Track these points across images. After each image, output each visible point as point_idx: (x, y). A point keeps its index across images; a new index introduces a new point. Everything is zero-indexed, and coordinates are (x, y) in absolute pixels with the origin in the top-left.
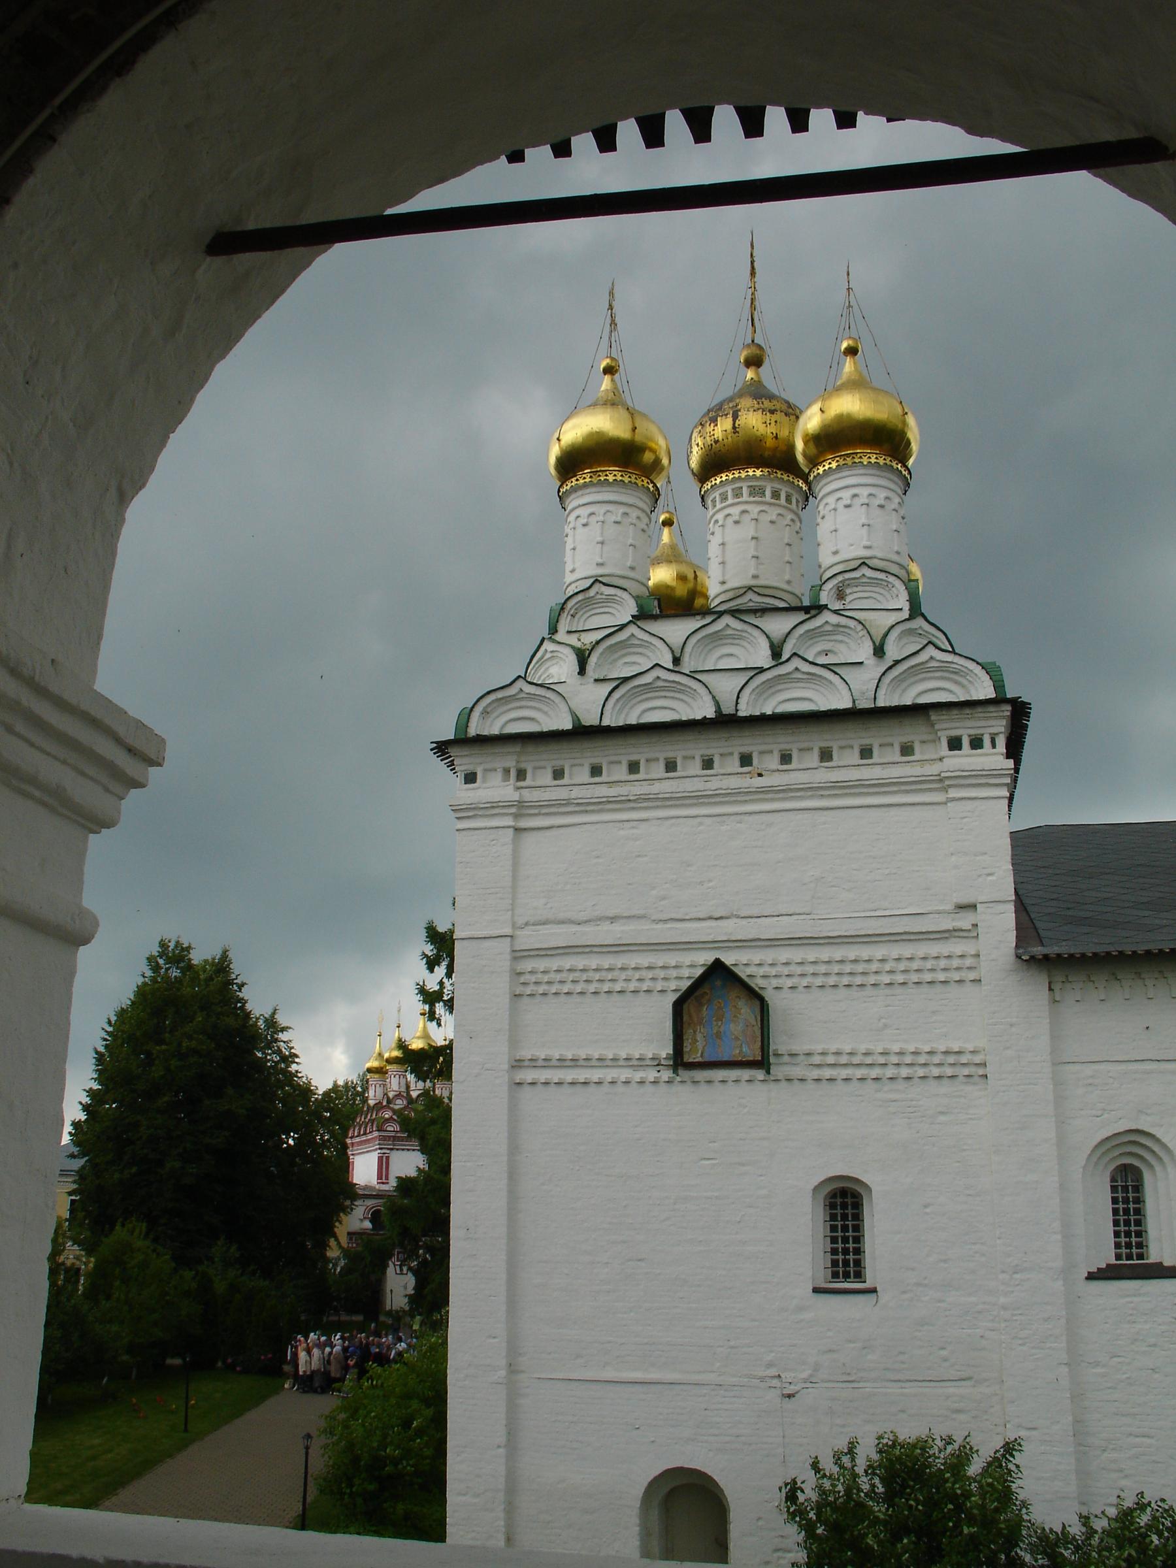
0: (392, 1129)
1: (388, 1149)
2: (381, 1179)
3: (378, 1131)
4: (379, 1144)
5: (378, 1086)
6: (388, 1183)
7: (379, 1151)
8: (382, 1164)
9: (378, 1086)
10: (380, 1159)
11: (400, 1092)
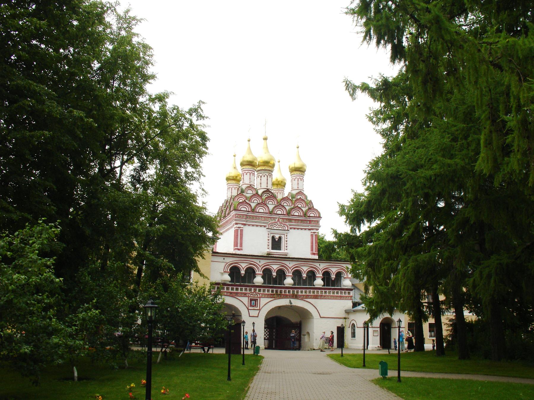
0: (245, 210)
1: (243, 224)
2: (237, 247)
3: (235, 210)
4: (236, 220)
5: (233, 189)
6: (242, 249)
7: (235, 226)
8: (237, 235)
9: (233, 189)
10: (236, 232)
11: (251, 185)
